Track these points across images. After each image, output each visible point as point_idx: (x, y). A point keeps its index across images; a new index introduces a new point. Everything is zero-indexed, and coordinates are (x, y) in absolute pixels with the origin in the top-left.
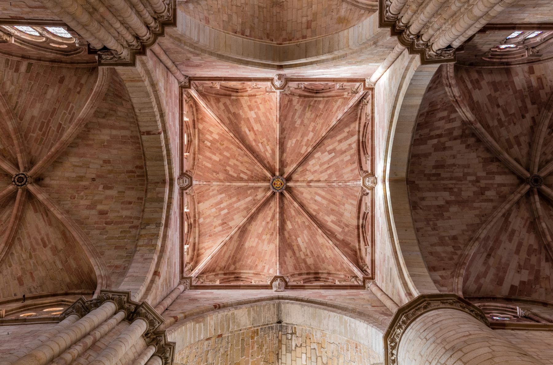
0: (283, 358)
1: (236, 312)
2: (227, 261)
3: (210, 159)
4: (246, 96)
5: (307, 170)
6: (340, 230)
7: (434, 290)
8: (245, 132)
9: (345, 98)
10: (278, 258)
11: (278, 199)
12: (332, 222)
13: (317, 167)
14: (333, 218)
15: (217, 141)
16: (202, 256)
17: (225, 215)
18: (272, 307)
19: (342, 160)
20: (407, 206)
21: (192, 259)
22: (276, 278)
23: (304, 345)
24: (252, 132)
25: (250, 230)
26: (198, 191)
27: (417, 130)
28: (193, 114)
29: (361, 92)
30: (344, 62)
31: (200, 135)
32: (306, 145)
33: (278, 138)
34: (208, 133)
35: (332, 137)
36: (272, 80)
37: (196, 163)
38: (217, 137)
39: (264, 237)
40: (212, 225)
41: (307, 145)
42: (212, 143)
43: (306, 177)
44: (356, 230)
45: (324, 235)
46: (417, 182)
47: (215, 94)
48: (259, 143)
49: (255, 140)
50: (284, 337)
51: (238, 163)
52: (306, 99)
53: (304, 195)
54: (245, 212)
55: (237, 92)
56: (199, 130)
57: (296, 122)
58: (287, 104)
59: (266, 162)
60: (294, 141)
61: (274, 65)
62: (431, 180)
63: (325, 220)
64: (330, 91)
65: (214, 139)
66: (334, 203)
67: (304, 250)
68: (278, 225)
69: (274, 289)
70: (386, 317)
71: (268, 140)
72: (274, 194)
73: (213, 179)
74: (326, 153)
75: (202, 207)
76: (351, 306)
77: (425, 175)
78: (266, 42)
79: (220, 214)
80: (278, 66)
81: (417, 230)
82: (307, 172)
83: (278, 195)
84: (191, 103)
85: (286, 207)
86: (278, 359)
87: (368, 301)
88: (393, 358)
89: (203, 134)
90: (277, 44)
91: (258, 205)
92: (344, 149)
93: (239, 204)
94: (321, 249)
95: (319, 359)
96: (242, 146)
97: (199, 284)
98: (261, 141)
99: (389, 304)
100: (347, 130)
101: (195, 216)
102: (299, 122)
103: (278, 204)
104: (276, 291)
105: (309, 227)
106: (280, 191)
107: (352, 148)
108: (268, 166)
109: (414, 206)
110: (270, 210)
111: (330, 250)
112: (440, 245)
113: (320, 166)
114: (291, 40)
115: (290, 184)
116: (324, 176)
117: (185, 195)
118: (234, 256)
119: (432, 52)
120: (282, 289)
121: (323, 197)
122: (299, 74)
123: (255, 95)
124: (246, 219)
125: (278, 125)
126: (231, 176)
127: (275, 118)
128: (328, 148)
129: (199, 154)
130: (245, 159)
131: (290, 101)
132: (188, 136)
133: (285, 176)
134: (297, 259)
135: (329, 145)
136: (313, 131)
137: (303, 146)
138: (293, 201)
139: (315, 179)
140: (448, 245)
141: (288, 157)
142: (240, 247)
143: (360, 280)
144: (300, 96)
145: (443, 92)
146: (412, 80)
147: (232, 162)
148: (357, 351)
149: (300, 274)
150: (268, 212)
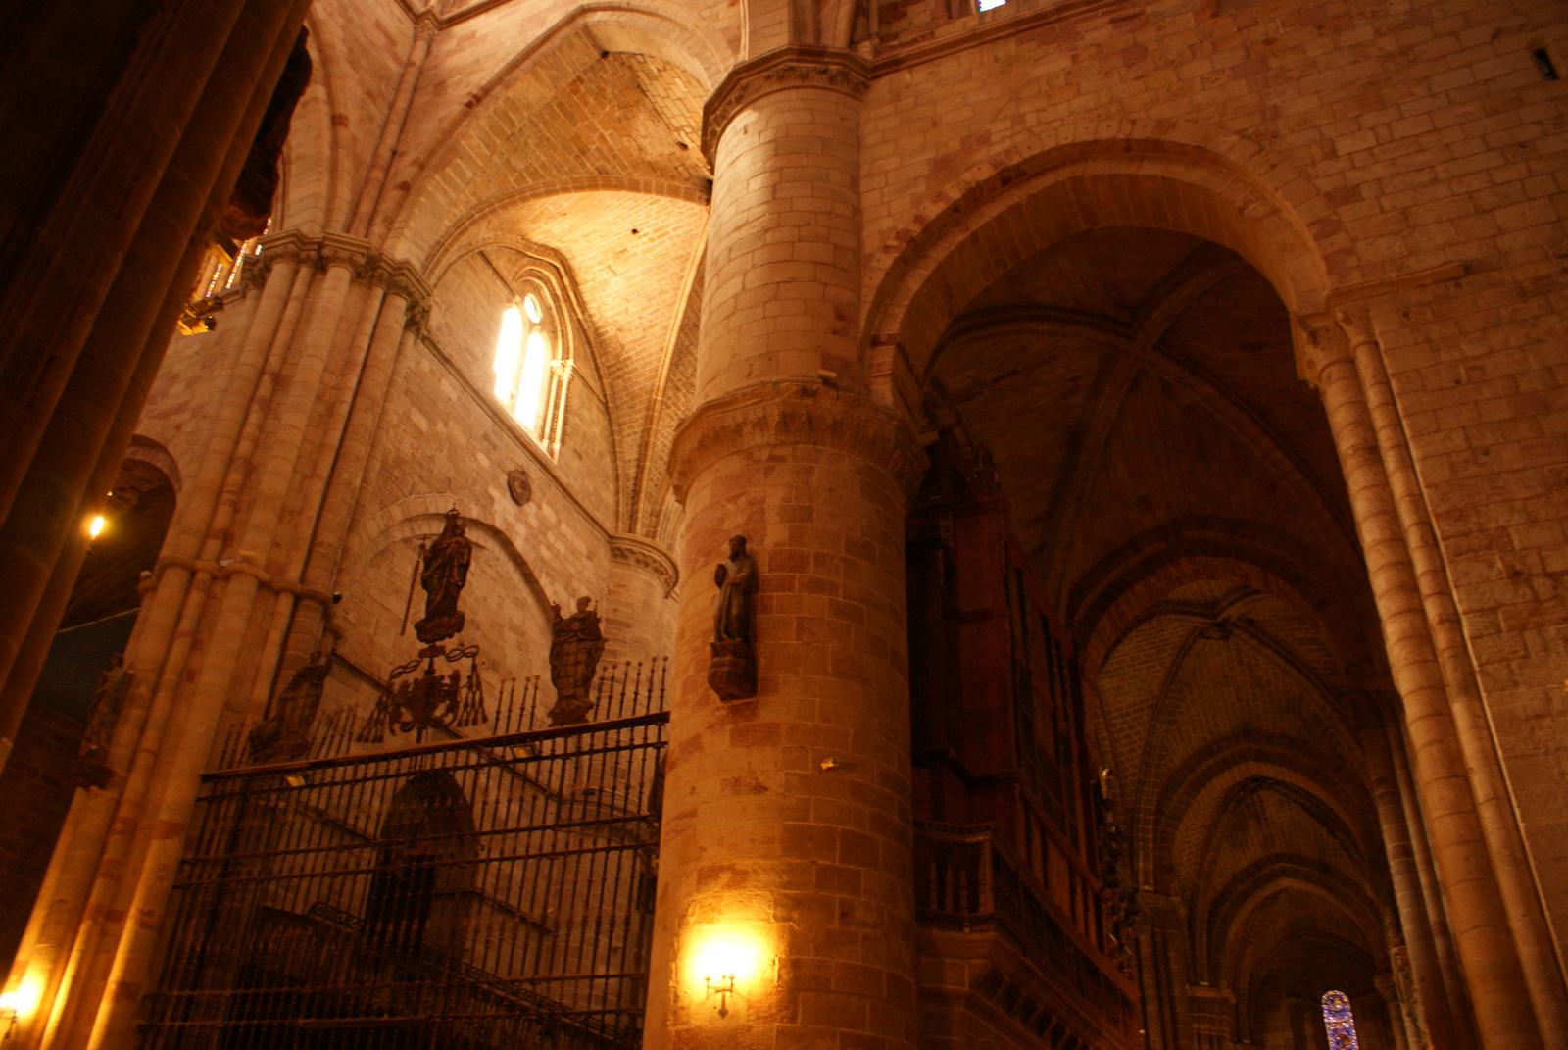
0: (650, 88)
1: (510, 93)
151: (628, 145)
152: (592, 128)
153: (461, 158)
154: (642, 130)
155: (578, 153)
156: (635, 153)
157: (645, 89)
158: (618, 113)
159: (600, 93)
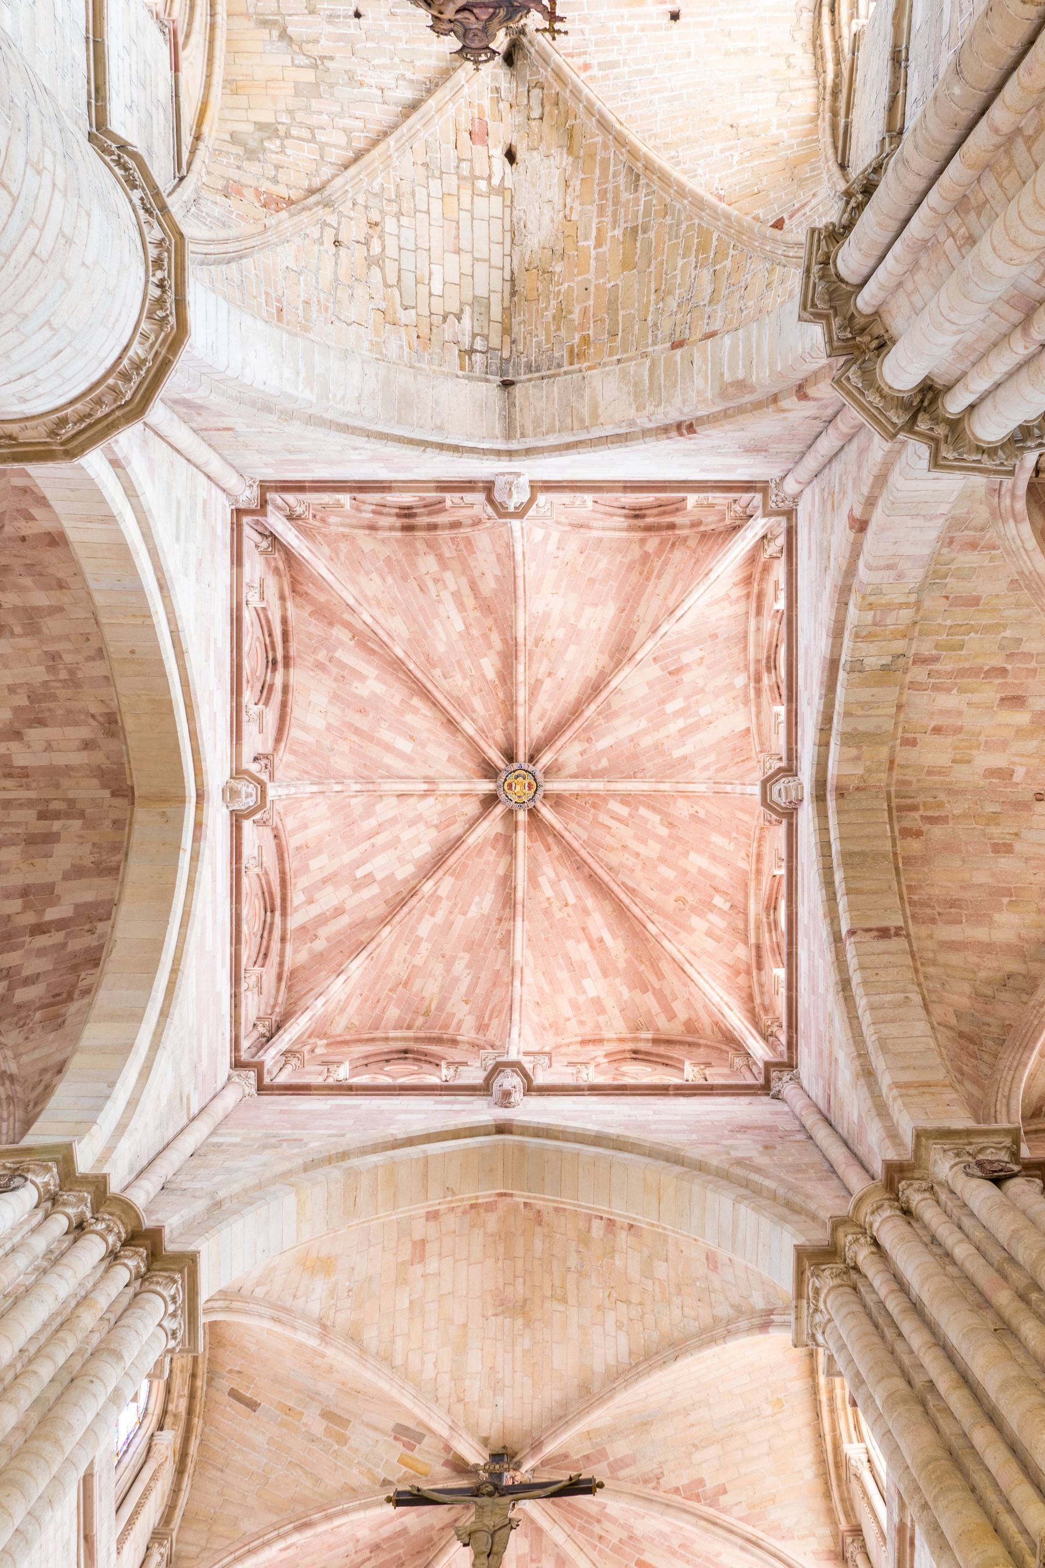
0: (497, 284)
2: (665, 563)
3: (714, 858)
4: (609, 1040)
5: (436, 826)
6: (339, 654)
7: (40, 473)
8: (614, 936)
9: (324, 1035)
10: (520, 573)
11: (521, 742)
12: (362, 678)
13: (406, 835)
14: (362, 690)
15: (693, 909)
16: (736, 579)
17: (672, 697)
18: (530, 428)
19: (333, 856)
20: (129, 723)
21: (766, 569)
22: (520, 513)
23: (437, 320)
24: (595, 936)
25: (601, 652)
26: (749, 765)
27: (101, 947)
28: (761, 986)
29: (270, 1057)
30: (312, 1145)
31: (741, 926)
32: (439, 898)
33: (519, 919)
34: (719, 932)
35: (362, 924)
36: (531, 1089)
37: (755, 845)
38: (695, 921)
39: (561, 633)
40: (709, 668)
41: (435, 898)
42: (710, 903)
43: (439, 808)
44: (293, 652)
45: (386, 638)
46: (106, 793)
47: (698, 1045)
48: (574, 905)
49: (586, 912)
50: (495, 341)
51: (635, 846)
52: (435, 1033)
53: (444, 755)
54: (615, 706)
55: (635, 1052)
56: (746, 942)
57: (468, 966)
58: (490, 1018)
59: (556, 850)
60: (473, 912)
61: (522, 1134)
62: (64, 800)
63: (385, 683)
64: (366, 1057)
65: (701, 915)
66: (357, 731)
67: (446, 596)
68: (521, 668)
69: (524, 481)
70: (188, 396)
71: (547, 912)
72: (532, 759)
73: (706, 798)
74: (379, 876)
75: (740, 719)
76: (295, 428)
77: (82, 814)
78: (544, 1200)
79: (687, 698)
80: (511, 1133)
81: (100, 653)
82: (436, 822)
83: (522, 754)
84: (765, 1019)
85: (499, 721)
86: (512, 280)
87: (246, 446)
88: (159, 274)
89: (735, 929)
90: (511, 1195)
91: (577, 725)
92: (329, 889)
93: (633, 729)
94: (395, 599)
95: (392, 280)
96: (622, 896)
97: (746, 497)
98: (570, 909)
99: (183, 436)
100: (320, 945)
101: (758, 692)
102: (459, 967)
103: (521, 729)
104: (518, 475)
105: (430, 662)
106: (515, 766)
107: (303, 890)
108: (550, 840)
109: (111, 724)
110: (545, 711)
111: (370, 594)
112: (37, 609)
113: (397, 839)
114: (472, 1206)
115: (486, 786)
116: (387, 809)
117: (784, 755)
118: (648, 579)
119: (39, 1180)
120: (500, 483)
121: (389, 748)
122: (448, 1107)
123: (584, 1042)
124: (613, 684)
125: (518, 957)
126: (654, 809)
127: (528, 979)
128: (374, 890)
129: (745, 873)
130: (613, 859)
131: (482, 1027)
132: (776, 922)
133: (499, 810)
134: (465, 569)
135: (372, 899)
136: (419, 940)
137: (448, 898)
138: (477, 738)
139: (412, 801)
140: (15, 609)
141: (492, 864)
142: (629, 604)
143: (278, 508)
144: (454, 1042)
145: (25, 1059)
146: (108, 1097)
147: (652, 850)
148: (279, 301)
149: (455, 525)
150: (549, 706)
151: (577, 205)
152: (601, 271)
153: (722, 375)
154: (546, 220)
155: (640, 236)
156: (576, 183)
157: (508, 285)
158: (558, 268)
159: (561, 315)
